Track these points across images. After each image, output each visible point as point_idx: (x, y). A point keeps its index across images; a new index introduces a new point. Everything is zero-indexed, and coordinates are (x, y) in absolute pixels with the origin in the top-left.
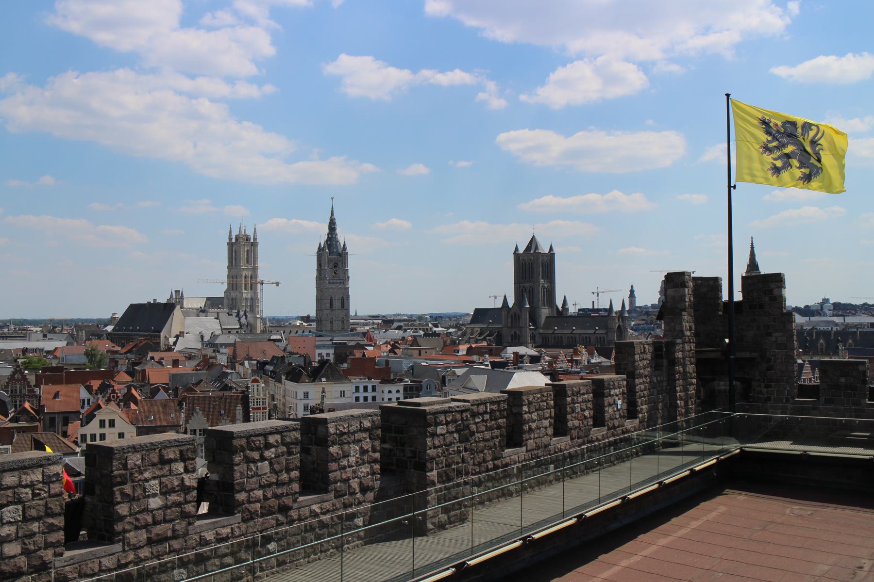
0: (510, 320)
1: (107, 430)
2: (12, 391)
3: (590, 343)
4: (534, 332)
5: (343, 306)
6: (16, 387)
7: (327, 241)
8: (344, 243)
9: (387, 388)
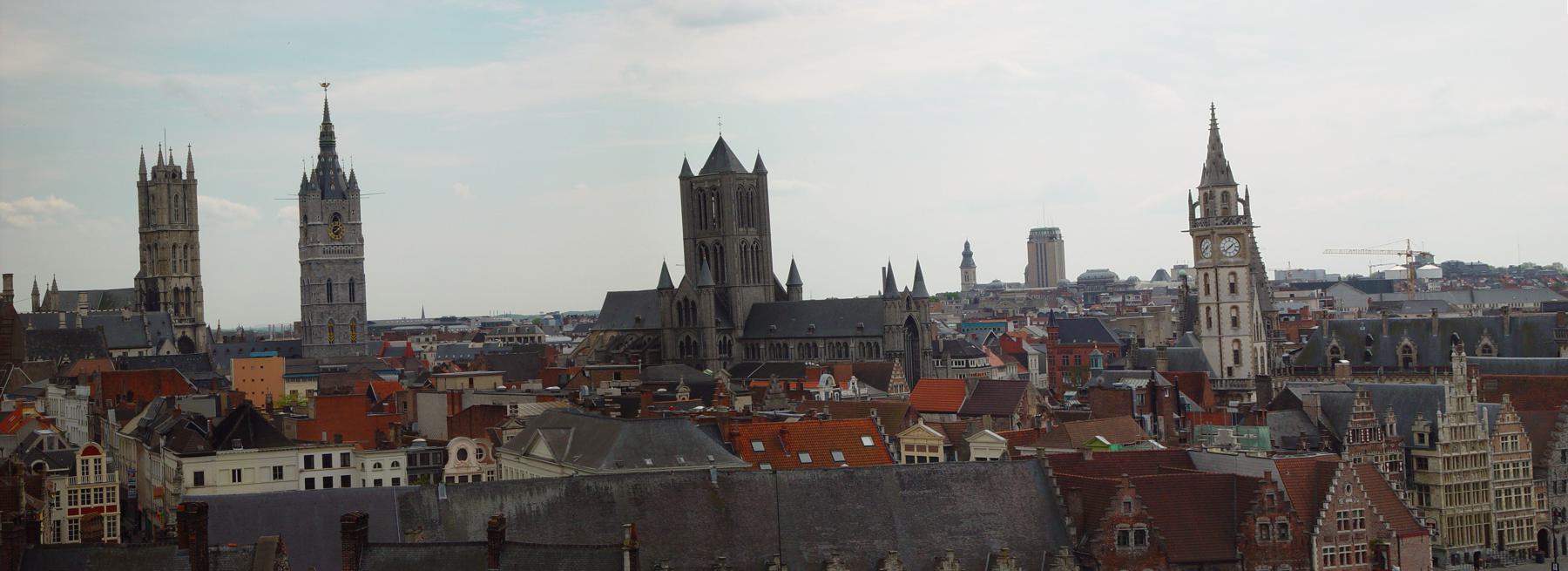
3: (847, 356)
4: (728, 338)
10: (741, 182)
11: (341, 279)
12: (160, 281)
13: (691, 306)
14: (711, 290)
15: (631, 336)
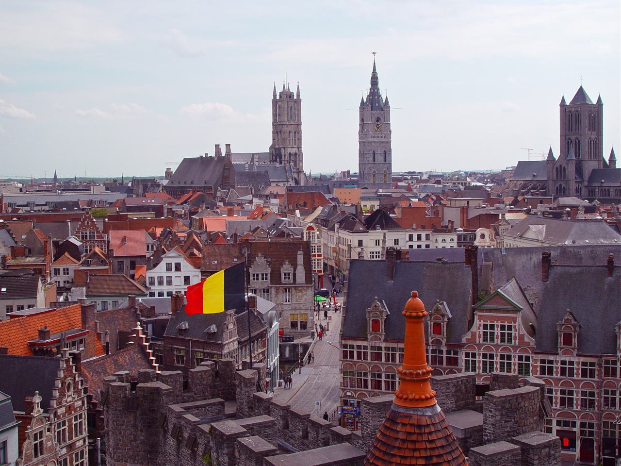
0: (555, 172)
1: (173, 274)
2: (83, 236)
4: (580, 186)
5: (385, 160)
6: (86, 233)
7: (369, 96)
8: (387, 98)
9: (440, 237)
10: (590, 109)
11: (380, 151)
12: (282, 149)
13: (563, 169)
14: (574, 162)
15: (530, 184)
